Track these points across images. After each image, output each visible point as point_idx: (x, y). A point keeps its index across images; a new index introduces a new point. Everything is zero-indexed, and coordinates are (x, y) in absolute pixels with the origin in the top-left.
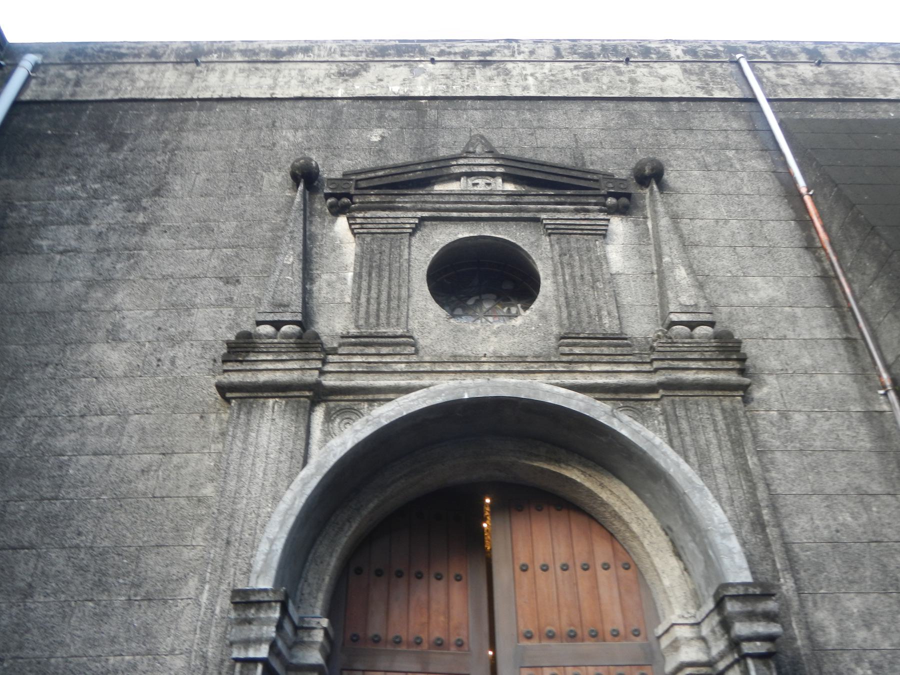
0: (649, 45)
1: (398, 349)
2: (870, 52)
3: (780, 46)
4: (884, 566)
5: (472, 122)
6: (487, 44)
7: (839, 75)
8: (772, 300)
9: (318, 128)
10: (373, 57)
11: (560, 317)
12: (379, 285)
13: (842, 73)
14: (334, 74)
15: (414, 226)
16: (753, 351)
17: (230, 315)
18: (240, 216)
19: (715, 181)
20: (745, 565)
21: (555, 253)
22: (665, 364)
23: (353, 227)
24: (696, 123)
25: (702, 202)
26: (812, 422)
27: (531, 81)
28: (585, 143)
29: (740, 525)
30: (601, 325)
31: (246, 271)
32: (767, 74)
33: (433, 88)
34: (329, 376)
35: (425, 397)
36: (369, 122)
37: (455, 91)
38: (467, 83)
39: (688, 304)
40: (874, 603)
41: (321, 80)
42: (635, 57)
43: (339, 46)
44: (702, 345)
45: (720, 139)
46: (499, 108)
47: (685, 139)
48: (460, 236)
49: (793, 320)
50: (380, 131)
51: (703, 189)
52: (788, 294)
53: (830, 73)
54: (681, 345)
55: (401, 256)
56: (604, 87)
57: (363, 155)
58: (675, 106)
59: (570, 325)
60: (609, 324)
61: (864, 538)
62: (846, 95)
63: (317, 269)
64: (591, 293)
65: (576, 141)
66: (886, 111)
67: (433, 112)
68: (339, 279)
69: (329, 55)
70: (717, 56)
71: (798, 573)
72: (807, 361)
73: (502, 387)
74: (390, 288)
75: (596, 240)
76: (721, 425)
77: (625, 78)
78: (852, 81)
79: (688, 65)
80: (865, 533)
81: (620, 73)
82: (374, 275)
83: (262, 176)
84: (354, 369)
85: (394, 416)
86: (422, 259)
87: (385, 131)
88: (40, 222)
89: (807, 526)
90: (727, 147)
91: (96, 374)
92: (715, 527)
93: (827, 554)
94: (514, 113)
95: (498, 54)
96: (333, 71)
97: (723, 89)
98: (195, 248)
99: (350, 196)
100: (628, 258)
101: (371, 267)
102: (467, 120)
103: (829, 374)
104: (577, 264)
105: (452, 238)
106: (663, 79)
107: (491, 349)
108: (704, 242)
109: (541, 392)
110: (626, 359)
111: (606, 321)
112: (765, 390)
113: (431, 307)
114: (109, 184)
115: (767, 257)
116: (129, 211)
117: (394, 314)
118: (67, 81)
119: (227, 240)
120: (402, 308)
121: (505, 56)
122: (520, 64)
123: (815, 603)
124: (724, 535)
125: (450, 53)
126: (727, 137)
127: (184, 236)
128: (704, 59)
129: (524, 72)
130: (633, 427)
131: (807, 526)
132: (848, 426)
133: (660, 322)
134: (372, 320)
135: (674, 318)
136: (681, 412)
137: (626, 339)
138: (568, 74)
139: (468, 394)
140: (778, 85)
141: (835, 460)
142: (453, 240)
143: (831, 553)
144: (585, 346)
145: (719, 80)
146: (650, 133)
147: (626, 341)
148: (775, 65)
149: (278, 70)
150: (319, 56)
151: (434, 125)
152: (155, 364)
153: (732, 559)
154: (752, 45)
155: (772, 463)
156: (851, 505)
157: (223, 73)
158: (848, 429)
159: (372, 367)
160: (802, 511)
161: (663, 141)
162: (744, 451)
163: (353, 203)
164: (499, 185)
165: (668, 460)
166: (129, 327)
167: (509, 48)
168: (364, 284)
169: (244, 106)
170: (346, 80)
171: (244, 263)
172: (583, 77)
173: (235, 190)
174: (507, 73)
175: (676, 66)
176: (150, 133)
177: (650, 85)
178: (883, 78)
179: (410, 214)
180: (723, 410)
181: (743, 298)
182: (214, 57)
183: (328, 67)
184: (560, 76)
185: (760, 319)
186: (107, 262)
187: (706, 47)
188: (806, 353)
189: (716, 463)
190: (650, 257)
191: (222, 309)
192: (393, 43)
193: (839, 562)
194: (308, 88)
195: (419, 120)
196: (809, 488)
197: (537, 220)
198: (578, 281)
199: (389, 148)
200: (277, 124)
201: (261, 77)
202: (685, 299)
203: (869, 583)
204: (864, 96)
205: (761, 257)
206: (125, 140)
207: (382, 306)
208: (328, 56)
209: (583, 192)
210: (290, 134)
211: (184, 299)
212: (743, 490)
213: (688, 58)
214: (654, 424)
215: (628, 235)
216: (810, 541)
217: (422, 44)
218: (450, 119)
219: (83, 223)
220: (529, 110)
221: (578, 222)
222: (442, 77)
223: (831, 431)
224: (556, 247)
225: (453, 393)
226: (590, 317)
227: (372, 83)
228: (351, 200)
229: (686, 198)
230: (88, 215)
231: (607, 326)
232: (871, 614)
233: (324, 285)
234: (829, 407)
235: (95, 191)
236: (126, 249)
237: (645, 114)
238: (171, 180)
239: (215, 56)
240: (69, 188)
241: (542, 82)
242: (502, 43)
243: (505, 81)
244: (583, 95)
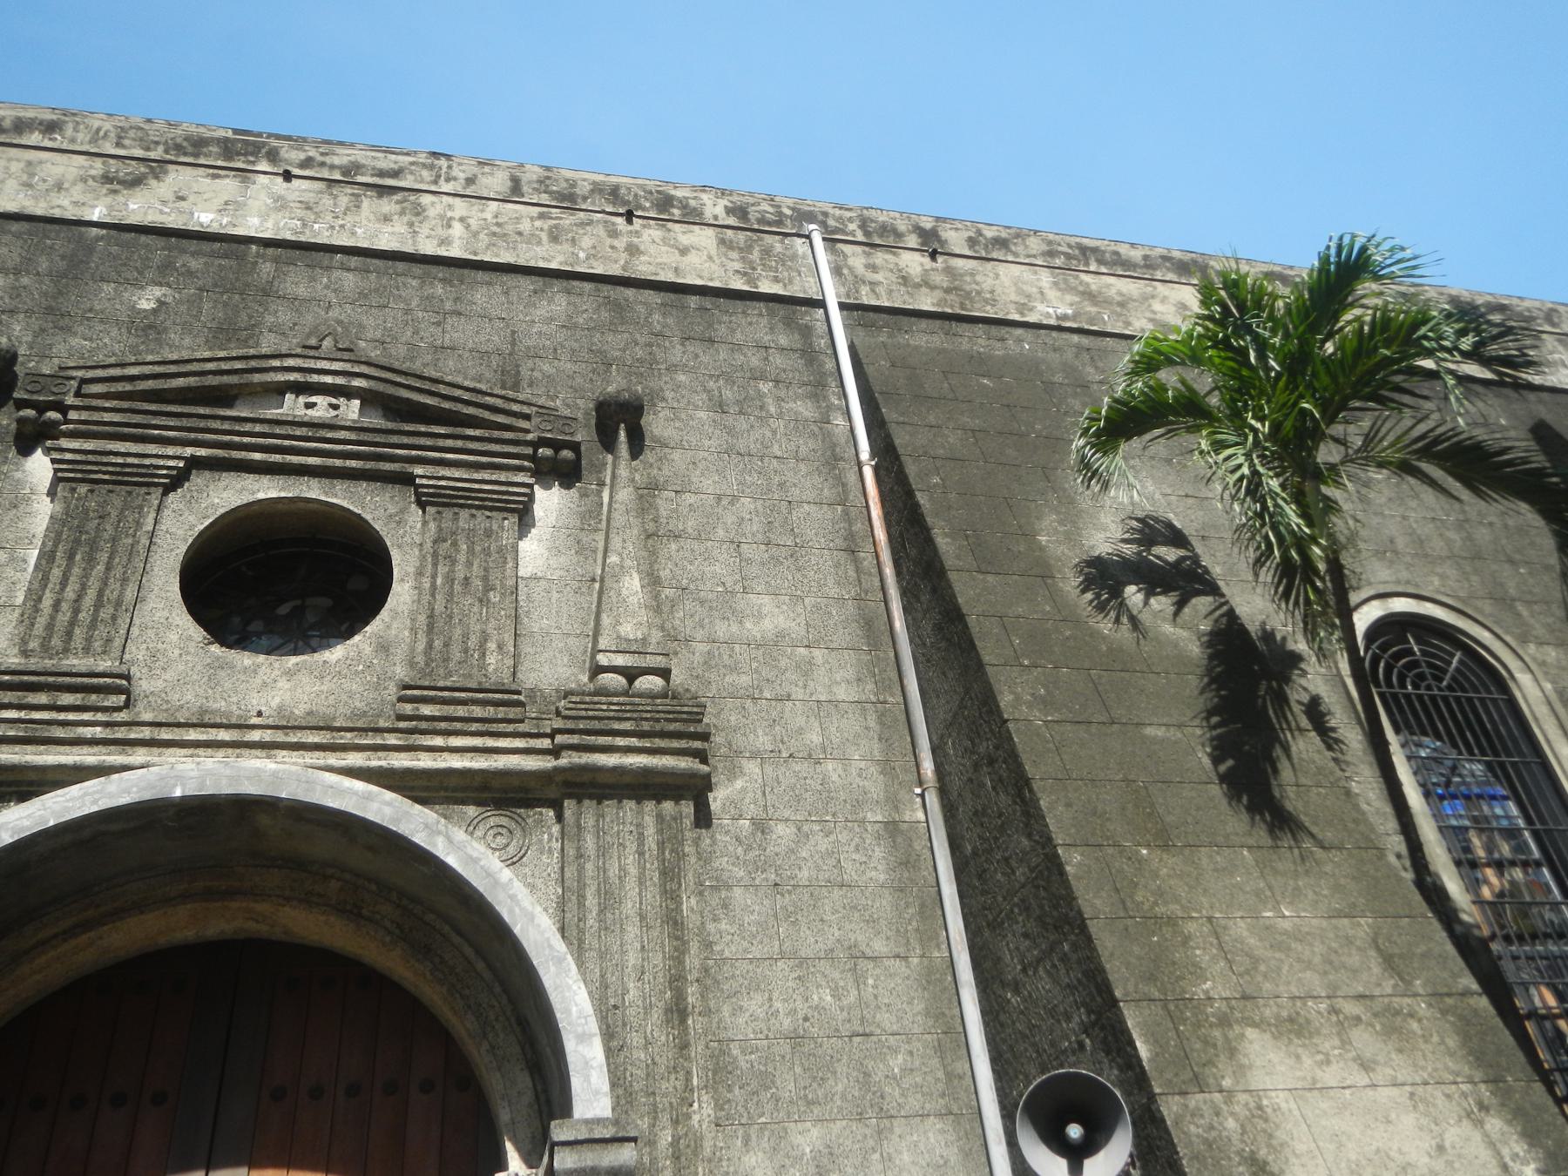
0: (673, 192)
1: (93, 699)
2: (1015, 244)
3: (881, 219)
4: (867, 1075)
5: (335, 291)
7: (962, 275)
8: (781, 635)
9: (38, 274)
11: (413, 650)
12: (86, 576)
13: (967, 273)
14: (93, 178)
16: (732, 718)
19: (731, 431)
20: (606, 1087)
21: (427, 535)
22: (574, 739)
24: (722, 330)
25: (701, 466)
26: (802, 836)
27: (457, 229)
28: (528, 348)
29: (645, 1013)
30: (483, 666)
32: (851, 261)
33: (277, 223)
35: (97, 792)
38: (341, 222)
39: (631, 637)
40: (838, 1137)
41: (66, 185)
42: (644, 209)
43: (116, 127)
44: (641, 708)
45: (755, 361)
46: (391, 271)
47: (697, 356)
48: (261, 496)
49: (806, 669)
50: (158, 292)
51: (707, 443)
52: (807, 624)
53: (948, 270)
54: (605, 707)
55: (139, 525)
56: (582, 255)
57: (114, 332)
58: (693, 301)
59: (427, 664)
60: (495, 665)
61: (845, 1030)
62: (963, 309)
64: (475, 609)
65: (513, 343)
66: (1019, 341)
67: (267, 268)
68: (12, 559)
69: (94, 140)
70: (779, 223)
71: (730, 1091)
72: (815, 738)
73: (248, 778)
74: (105, 583)
75: (505, 519)
76: (651, 842)
77: (620, 243)
78: (977, 288)
79: (729, 232)
80: (849, 1021)
81: (614, 234)
82: (78, 557)
85: (28, 828)
86: (180, 532)
87: (170, 292)
89: (760, 1013)
90: (763, 378)
92: (569, 1024)
93: (783, 1057)
94: (414, 283)
95: (409, 176)
96: (93, 172)
97: (776, 280)
99: (63, 409)
100: (556, 551)
101: (77, 542)
102: (327, 287)
103: (845, 760)
104: (462, 558)
105: (246, 498)
106: (684, 251)
107: (275, 703)
108: (690, 531)
109: (319, 788)
110: (510, 728)
111: (492, 659)
112: (739, 784)
113: (178, 621)
115: (786, 563)
117: (101, 631)
120: (119, 621)
121: (422, 181)
122: (445, 198)
123: (746, 1141)
124: (583, 1038)
125: (323, 164)
126: (766, 359)
128: (756, 227)
129: (449, 214)
130: (469, 850)
131: (760, 1013)
132: (857, 845)
133: (587, 665)
134: (56, 642)
135: (603, 660)
136: (589, 820)
137: (519, 693)
138: (525, 226)
139: (183, 791)
140: (864, 282)
141: (826, 901)
142: (245, 502)
143: (788, 1057)
144: (445, 702)
145: (774, 264)
146: (641, 340)
147: (516, 697)
148: (867, 249)
150: (73, 141)
151: (263, 290)
153: (587, 1079)
154: (838, 212)
155: (725, 906)
156: (837, 975)
158: (857, 849)
159: (36, 730)
160: (755, 986)
161: (660, 356)
162: (680, 885)
163: (67, 422)
164: (351, 410)
165: (517, 910)
167: (431, 167)
168: (56, 573)
170: (115, 192)
172: (550, 233)
174: (419, 211)
175: (710, 232)
177: (659, 260)
178: (1025, 287)
179: (170, 450)
180: (660, 818)
181: (734, 628)
183: (87, 164)
184: (511, 227)
185: (754, 665)
187: (765, 207)
188: (817, 724)
189: (629, 907)
190: (595, 551)
192: (221, 133)
193: (798, 1070)
194: (35, 198)
195: (237, 279)
196: (776, 949)
197: (407, 480)
198: (457, 588)
199: (168, 323)
202: (628, 629)
203: (839, 1103)
204: (990, 312)
205: (777, 561)
207: (81, 616)
208: (90, 142)
209: (496, 434)
212: (664, 952)
213: (732, 221)
214: (541, 841)
215: (565, 511)
216: (759, 1036)
217: (274, 143)
218: (297, 282)
220: (443, 280)
221: (476, 486)
223: (830, 854)
224: (432, 526)
225: (154, 788)
226: (466, 651)
227: (164, 202)
228: (65, 414)
229: (676, 455)
231: (491, 669)
232: (831, 1154)
234: (834, 815)
237: (641, 309)
241: (475, 234)
242: (422, 158)
243: (411, 225)
244: (542, 264)
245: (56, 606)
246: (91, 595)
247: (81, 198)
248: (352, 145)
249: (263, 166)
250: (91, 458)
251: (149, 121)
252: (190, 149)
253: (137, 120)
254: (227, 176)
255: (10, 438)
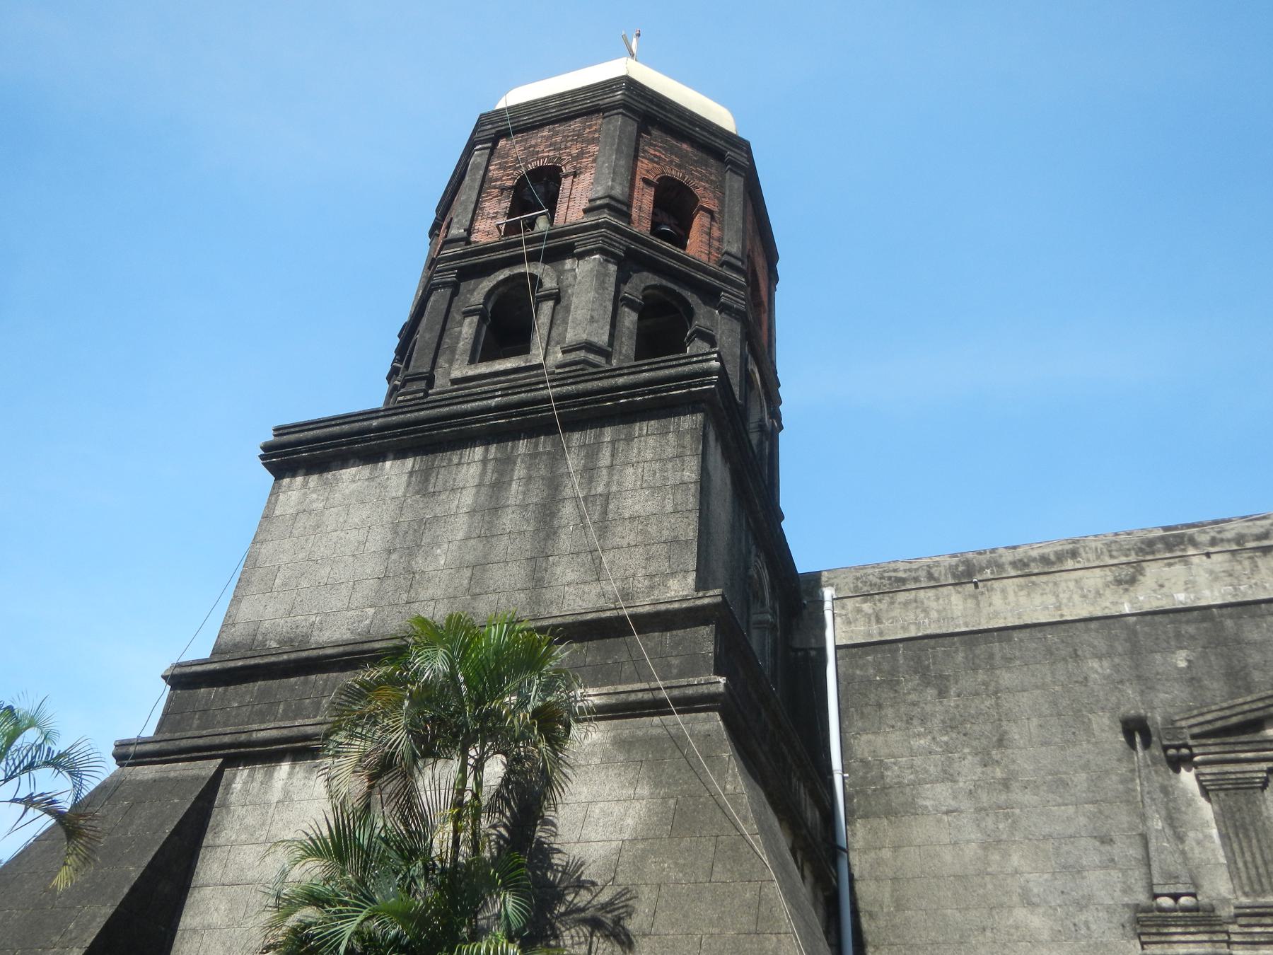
6: (1258, 523)
10: (1144, 556)
12: (1250, 846)
14: (1111, 582)
15: (1263, 780)
17: (1118, 877)
18: (1086, 767)
23: (1202, 778)
31: (1114, 828)
34: (1236, 946)
36: (1168, 643)
37: (1245, 594)
41: (1101, 592)
63: (1181, 827)
67: (1229, 623)
69: (1098, 557)
82: (1241, 836)
83: (1089, 719)
84: (1257, 939)
88: (915, 781)
91: (1028, 938)
98: (1059, 805)
99: (1189, 748)
101: (1235, 826)
114: (954, 735)
116: (985, 766)
118: (868, 616)
119: (1084, 795)
127: (1044, 791)
134: (1257, 887)
149: (1055, 584)
152: (1073, 929)
157: (1003, 591)
166: (1035, 891)
168: (1236, 846)
169: (1039, 632)
170: (1126, 590)
171: (1110, 821)
173: (1070, 736)
176: (966, 673)
179: (1256, 766)
182: (988, 573)
186: (989, 822)
191: (1109, 871)
200: (1080, 653)
201: (1042, 594)
206: (948, 683)
210: (1095, 664)
211: (1071, 861)
217: (1189, 531)
219: (951, 781)
222: (1223, 574)
230: (952, 771)
233: (1194, 844)
235: (946, 743)
236: (1000, 807)
238: (1007, 728)
239: (989, 571)
240: (922, 742)
245: (1247, 868)
246: (1258, 856)
247: (1112, 599)
248: (1229, 520)
249: (1191, 551)
250: (1219, 777)
251: (1116, 534)
252: (1148, 549)
253: (1111, 538)
254: (1175, 563)
255: (1165, 763)
